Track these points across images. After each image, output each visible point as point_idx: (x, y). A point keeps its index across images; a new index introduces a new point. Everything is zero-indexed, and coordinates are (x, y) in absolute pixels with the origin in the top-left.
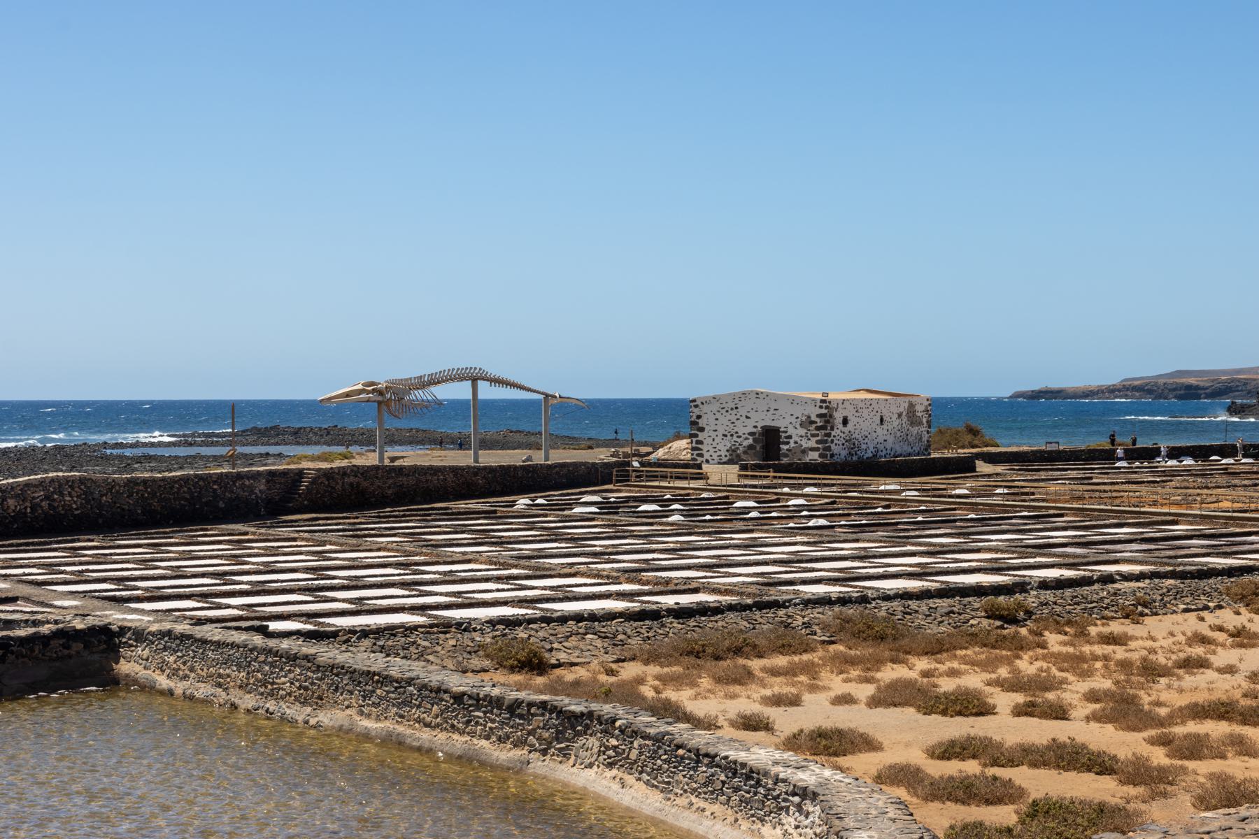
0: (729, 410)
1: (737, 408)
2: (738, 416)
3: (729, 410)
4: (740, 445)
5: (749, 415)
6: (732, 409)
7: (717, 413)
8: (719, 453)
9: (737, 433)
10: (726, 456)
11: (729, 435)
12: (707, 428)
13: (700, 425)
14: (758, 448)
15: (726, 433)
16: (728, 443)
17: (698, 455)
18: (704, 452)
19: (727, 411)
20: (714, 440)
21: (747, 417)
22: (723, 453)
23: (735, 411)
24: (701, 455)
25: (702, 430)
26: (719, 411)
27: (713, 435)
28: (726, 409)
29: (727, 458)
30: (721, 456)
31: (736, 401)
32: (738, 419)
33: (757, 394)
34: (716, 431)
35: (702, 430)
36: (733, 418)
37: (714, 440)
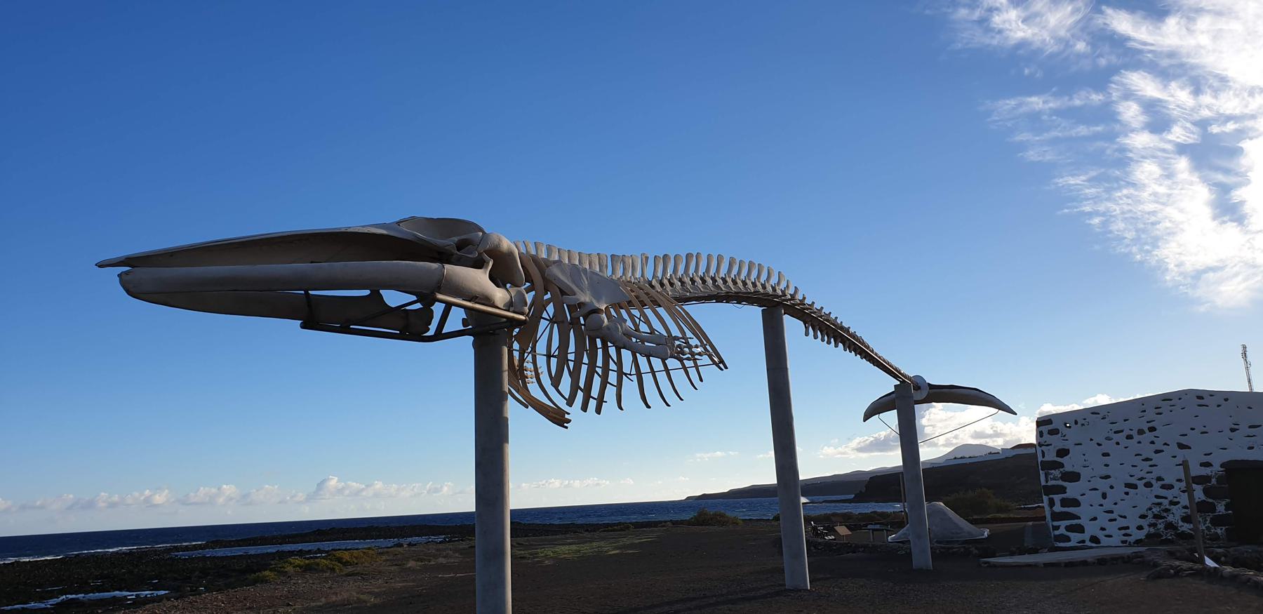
0: (1134, 433)
1: (1152, 429)
2: (1159, 446)
3: (1134, 433)
4: (1172, 503)
5: (1183, 440)
6: (1141, 432)
7: (1105, 443)
8: (1123, 523)
9: (1159, 479)
10: (1140, 528)
11: (1140, 484)
12: (1085, 474)
13: (1068, 468)
14: (1221, 508)
15: (1133, 481)
16: (1144, 499)
17: (1068, 528)
18: (1083, 521)
19: (1129, 437)
20: (1104, 496)
21: (1181, 446)
22: (1133, 521)
23: (1149, 436)
24: (1080, 529)
25: (1074, 477)
26: (1108, 439)
27: (1103, 485)
28: (1127, 432)
29: (1145, 532)
30: (1127, 528)
31: (1151, 414)
32: (1157, 452)
33: (1200, 398)
34: (1108, 477)
35: (1074, 477)
36: (1148, 451)
37: (1104, 496)
